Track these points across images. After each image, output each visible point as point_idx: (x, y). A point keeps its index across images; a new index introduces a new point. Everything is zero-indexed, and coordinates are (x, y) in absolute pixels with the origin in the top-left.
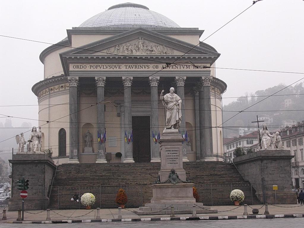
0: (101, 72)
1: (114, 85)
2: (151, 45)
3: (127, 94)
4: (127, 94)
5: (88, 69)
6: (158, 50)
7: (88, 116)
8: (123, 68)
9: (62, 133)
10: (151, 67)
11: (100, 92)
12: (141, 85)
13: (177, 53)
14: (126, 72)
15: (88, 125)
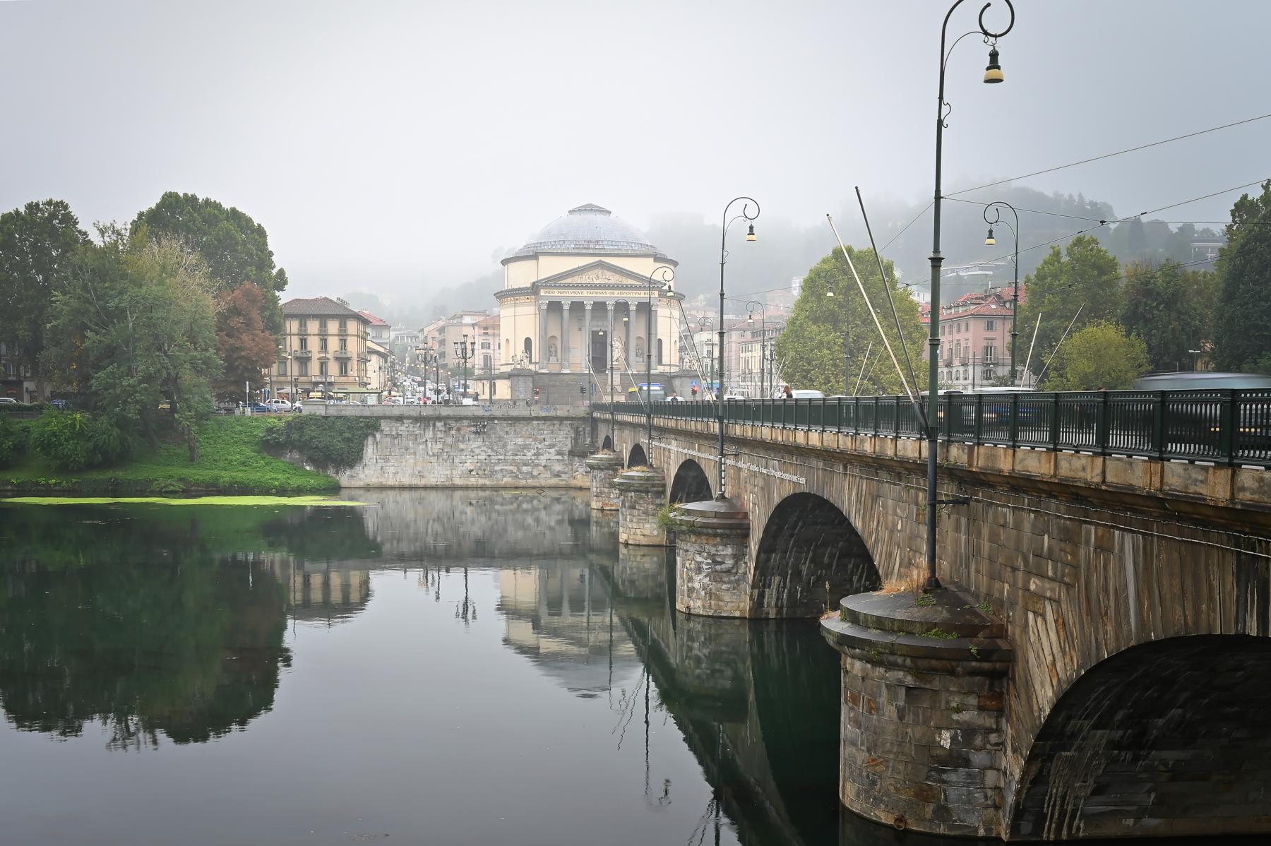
0: (566, 297)
1: (577, 307)
2: (608, 274)
3: (588, 316)
4: (588, 316)
5: (556, 294)
6: (614, 279)
7: (554, 331)
8: (585, 293)
9: (528, 342)
10: (608, 293)
11: (566, 314)
12: (600, 307)
13: (630, 281)
14: (588, 297)
15: (553, 337)
